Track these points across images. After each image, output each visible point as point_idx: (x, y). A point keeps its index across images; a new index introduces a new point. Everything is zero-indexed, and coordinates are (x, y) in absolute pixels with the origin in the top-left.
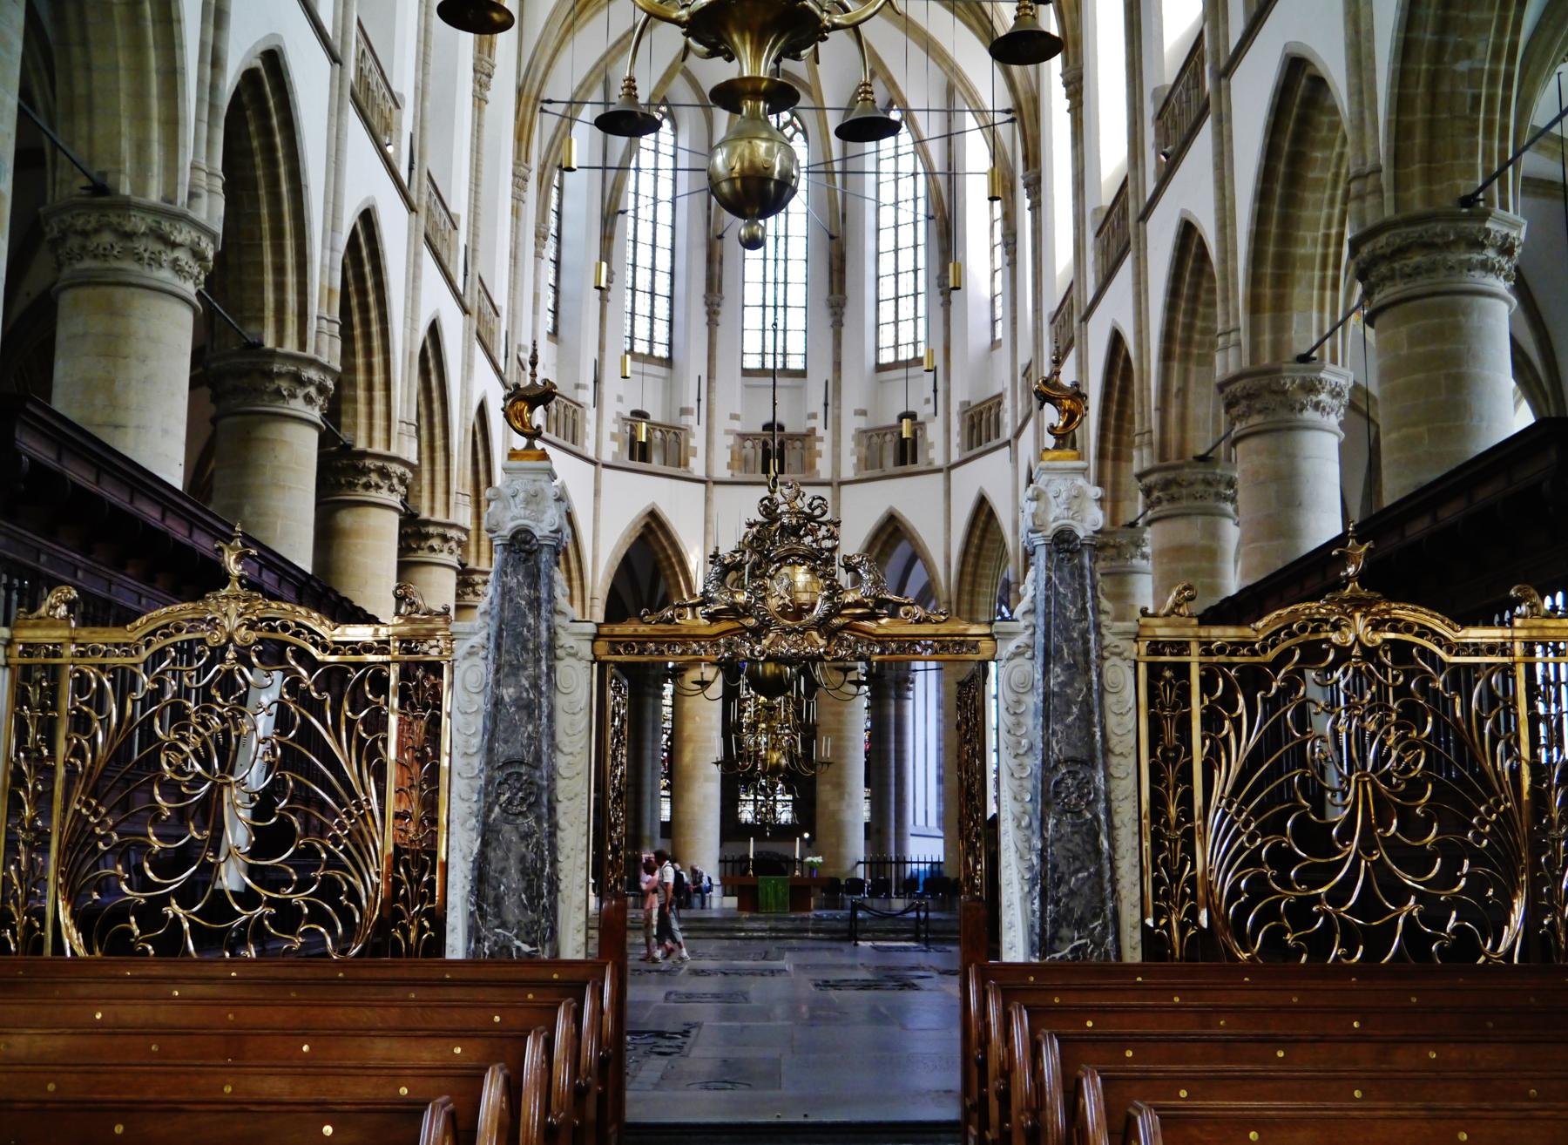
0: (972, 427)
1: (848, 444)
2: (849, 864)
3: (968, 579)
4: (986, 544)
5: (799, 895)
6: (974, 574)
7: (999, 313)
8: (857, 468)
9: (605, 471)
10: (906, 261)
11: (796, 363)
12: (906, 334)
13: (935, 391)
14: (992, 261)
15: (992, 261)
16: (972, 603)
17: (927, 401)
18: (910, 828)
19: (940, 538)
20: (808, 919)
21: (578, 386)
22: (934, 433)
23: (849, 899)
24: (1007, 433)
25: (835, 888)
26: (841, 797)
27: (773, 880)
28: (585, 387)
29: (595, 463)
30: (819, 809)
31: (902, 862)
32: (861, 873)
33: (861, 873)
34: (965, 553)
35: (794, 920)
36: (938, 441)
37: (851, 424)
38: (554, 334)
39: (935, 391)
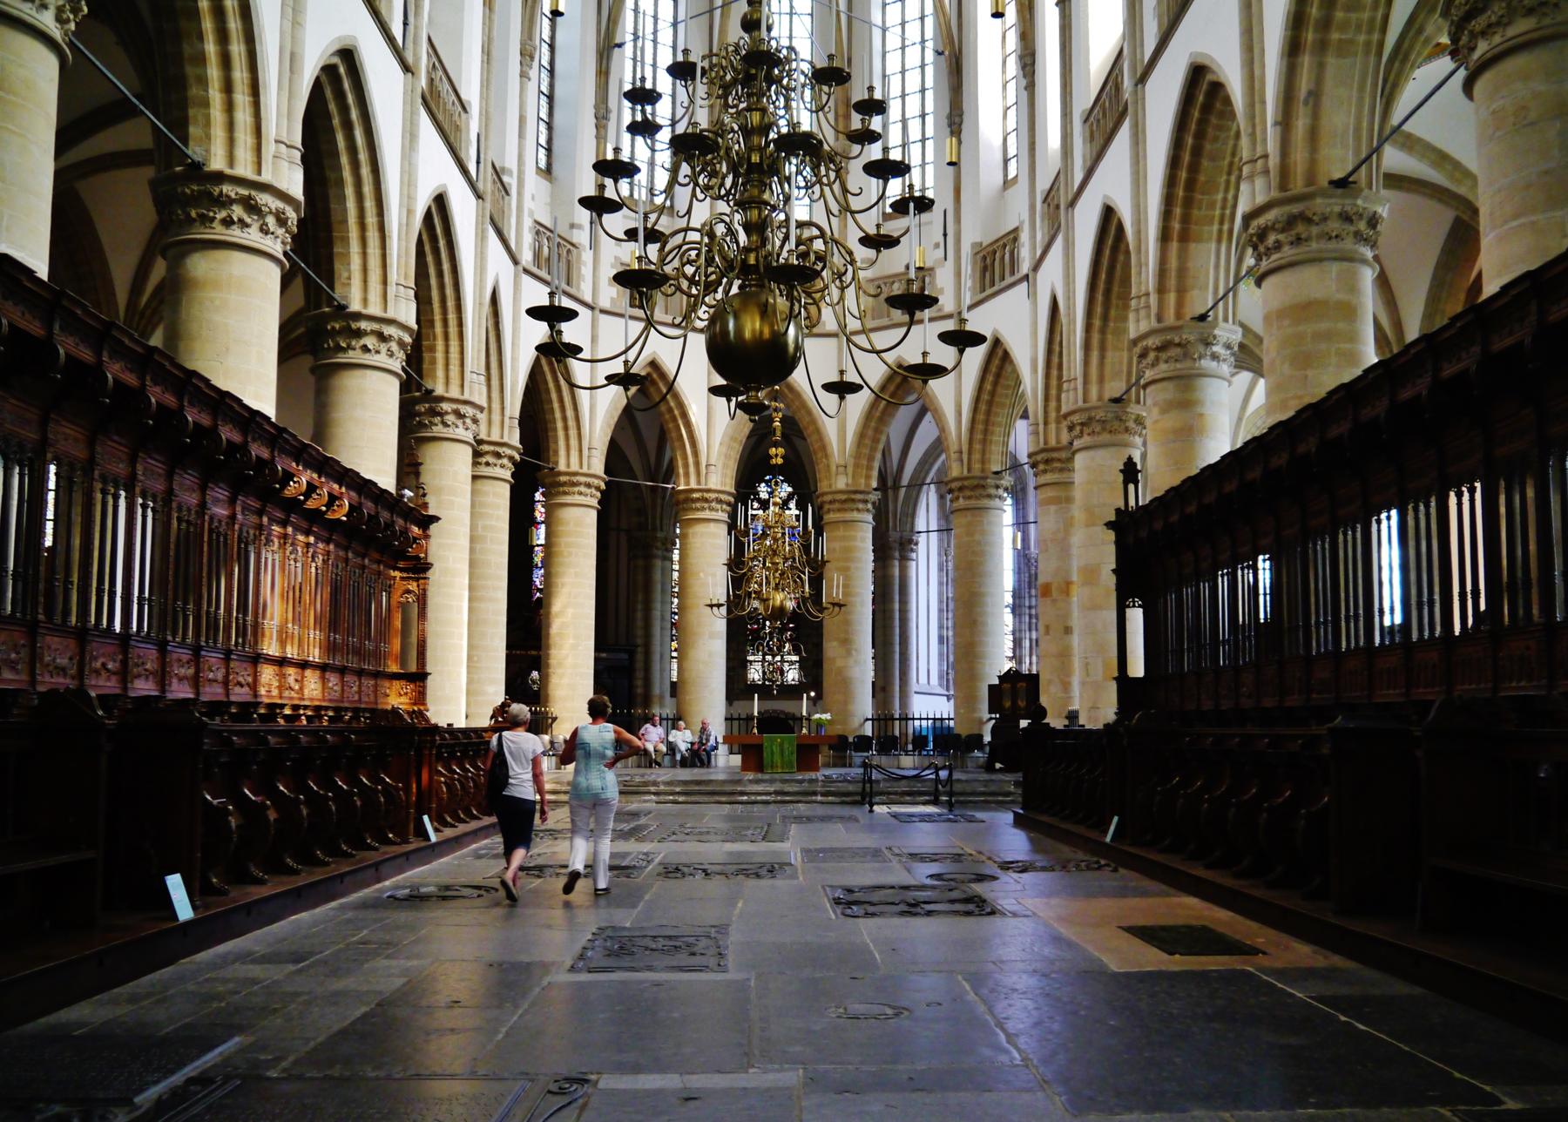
0: (985, 269)
2: (856, 722)
3: (980, 427)
4: (999, 390)
5: (806, 756)
6: (987, 422)
7: (1012, 151)
9: (603, 318)
13: (945, 235)
14: (1005, 98)
15: (1005, 98)
16: (984, 452)
17: (937, 246)
18: (914, 687)
20: (816, 780)
21: (572, 226)
23: (858, 757)
24: (1025, 268)
25: (842, 747)
26: (849, 653)
27: (779, 737)
28: (580, 227)
29: (592, 308)
30: (825, 666)
31: (905, 718)
32: (868, 730)
33: (868, 730)
34: (977, 400)
35: (801, 782)
38: (548, 172)
39: (945, 235)
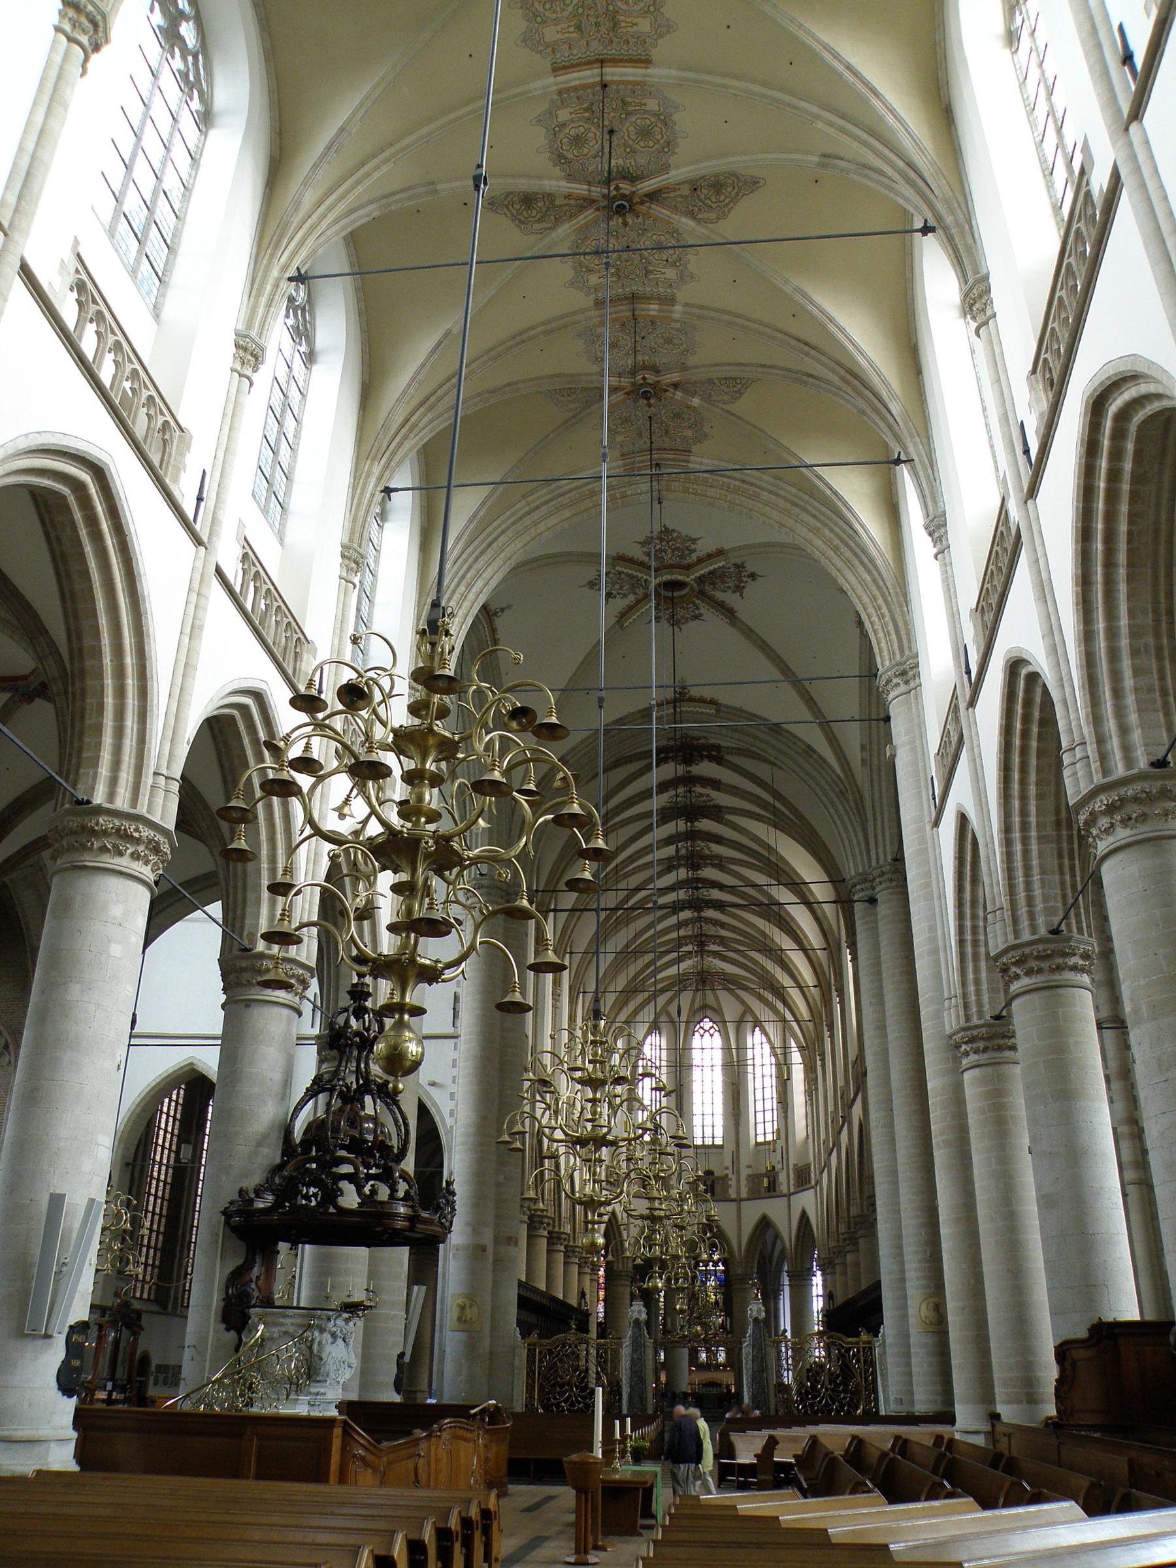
1: (743, 1182)
8: (748, 1193)
10: (768, 1094)
11: (719, 1142)
12: (769, 1129)
19: (787, 1229)
22: (782, 1177)
24: (813, 1183)
34: (798, 1236)
36: (785, 1181)
37: (745, 1172)
